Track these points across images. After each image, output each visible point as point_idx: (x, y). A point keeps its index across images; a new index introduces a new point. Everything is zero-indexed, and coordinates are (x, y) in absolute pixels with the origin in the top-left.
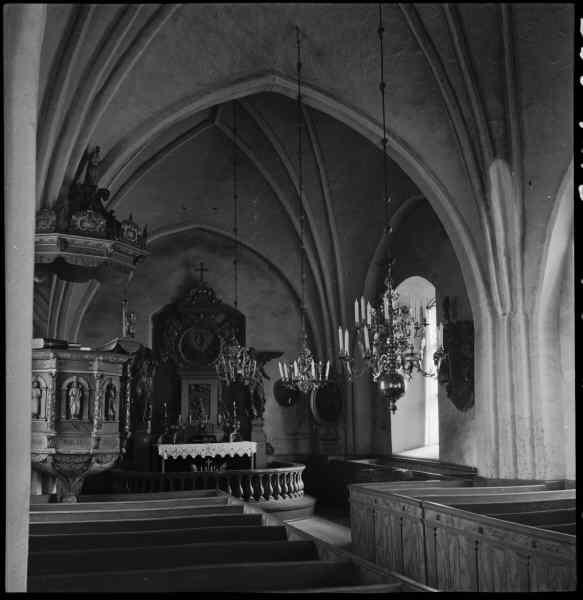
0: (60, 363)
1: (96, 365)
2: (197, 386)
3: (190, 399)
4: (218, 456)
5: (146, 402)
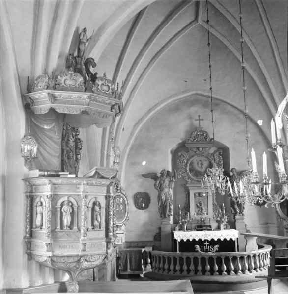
0: (54, 186)
1: (81, 188)
2: (199, 194)
3: (195, 202)
4: (213, 240)
5: (168, 204)
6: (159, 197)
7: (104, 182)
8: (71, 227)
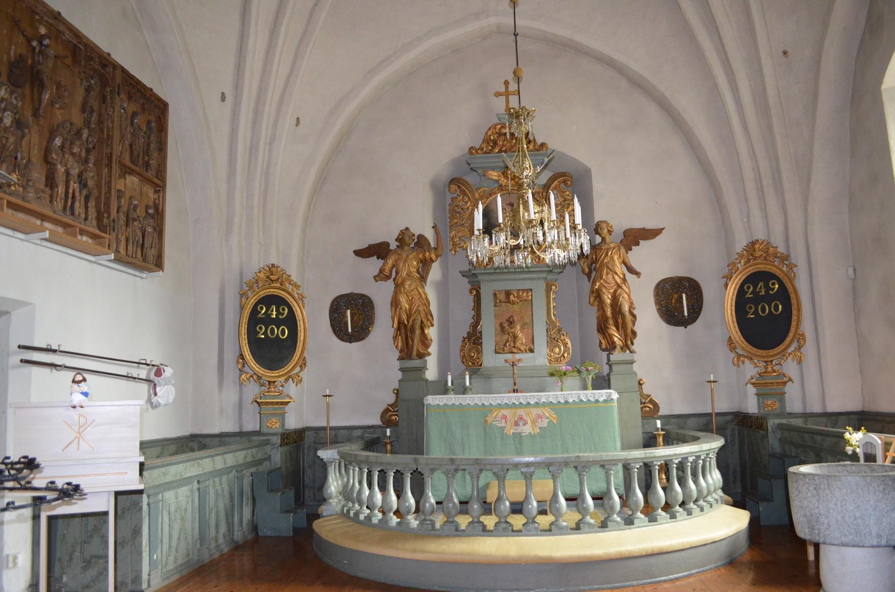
2: (508, 293)
6: (395, 303)
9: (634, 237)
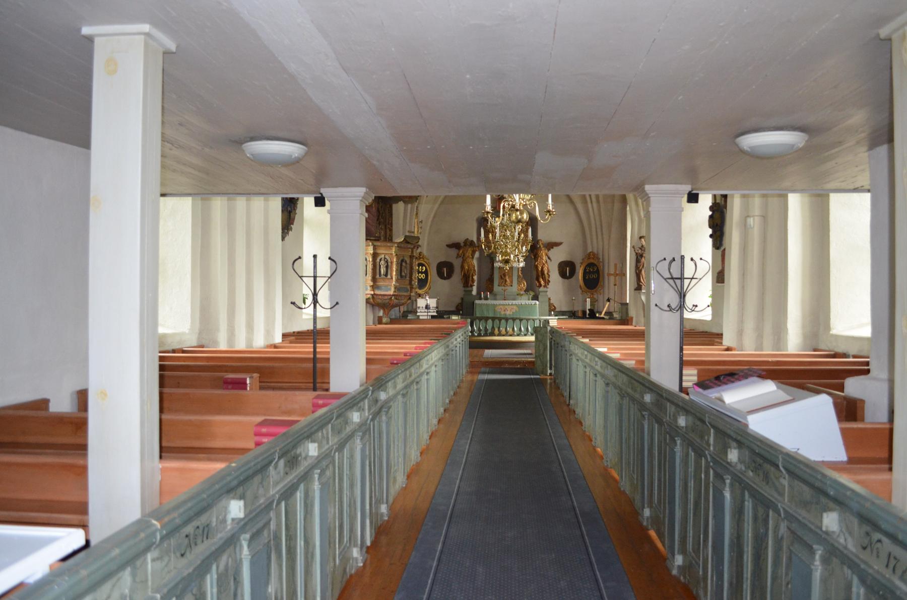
6: (462, 267)
7: (409, 246)
8: (386, 275)
9: (550, 246)
